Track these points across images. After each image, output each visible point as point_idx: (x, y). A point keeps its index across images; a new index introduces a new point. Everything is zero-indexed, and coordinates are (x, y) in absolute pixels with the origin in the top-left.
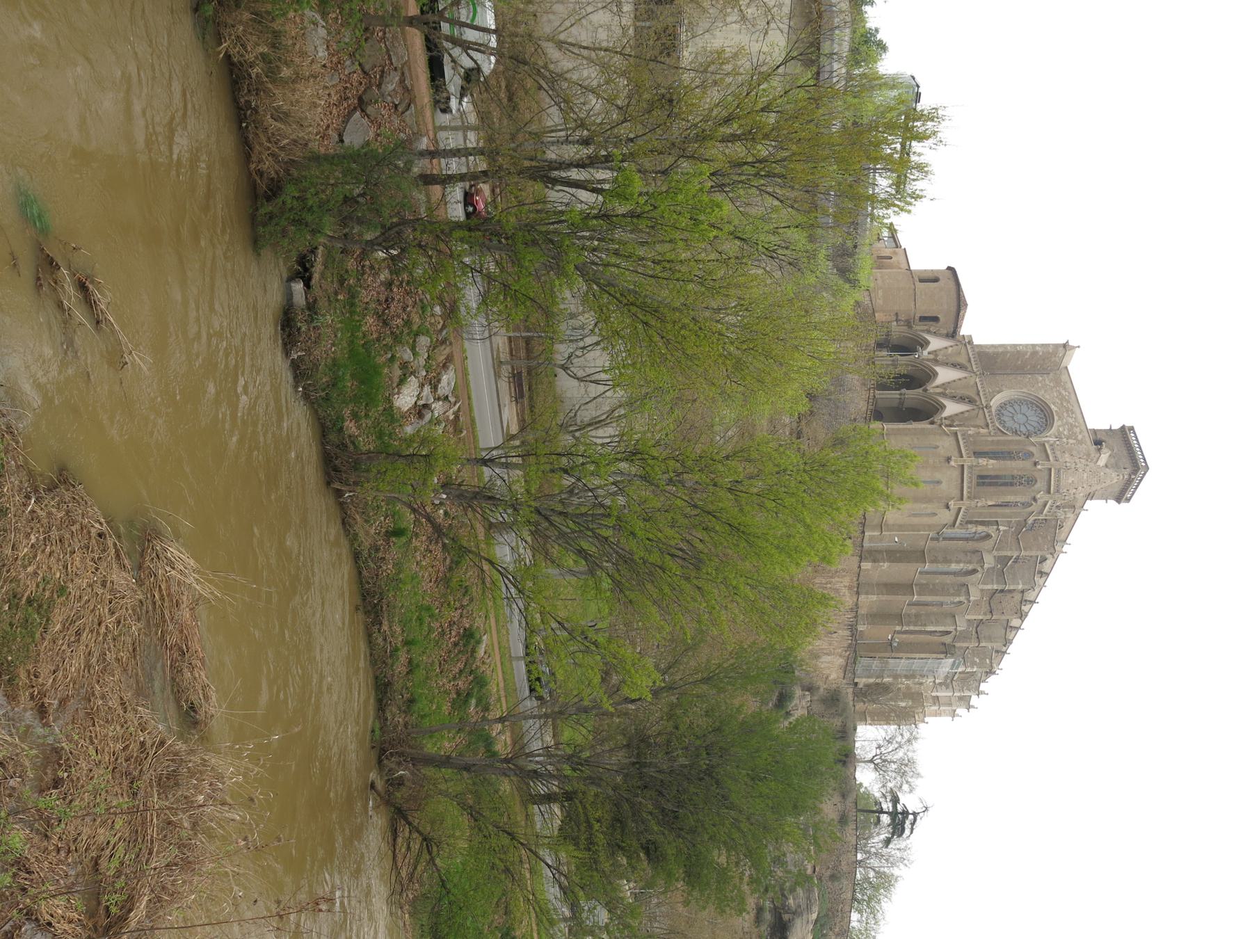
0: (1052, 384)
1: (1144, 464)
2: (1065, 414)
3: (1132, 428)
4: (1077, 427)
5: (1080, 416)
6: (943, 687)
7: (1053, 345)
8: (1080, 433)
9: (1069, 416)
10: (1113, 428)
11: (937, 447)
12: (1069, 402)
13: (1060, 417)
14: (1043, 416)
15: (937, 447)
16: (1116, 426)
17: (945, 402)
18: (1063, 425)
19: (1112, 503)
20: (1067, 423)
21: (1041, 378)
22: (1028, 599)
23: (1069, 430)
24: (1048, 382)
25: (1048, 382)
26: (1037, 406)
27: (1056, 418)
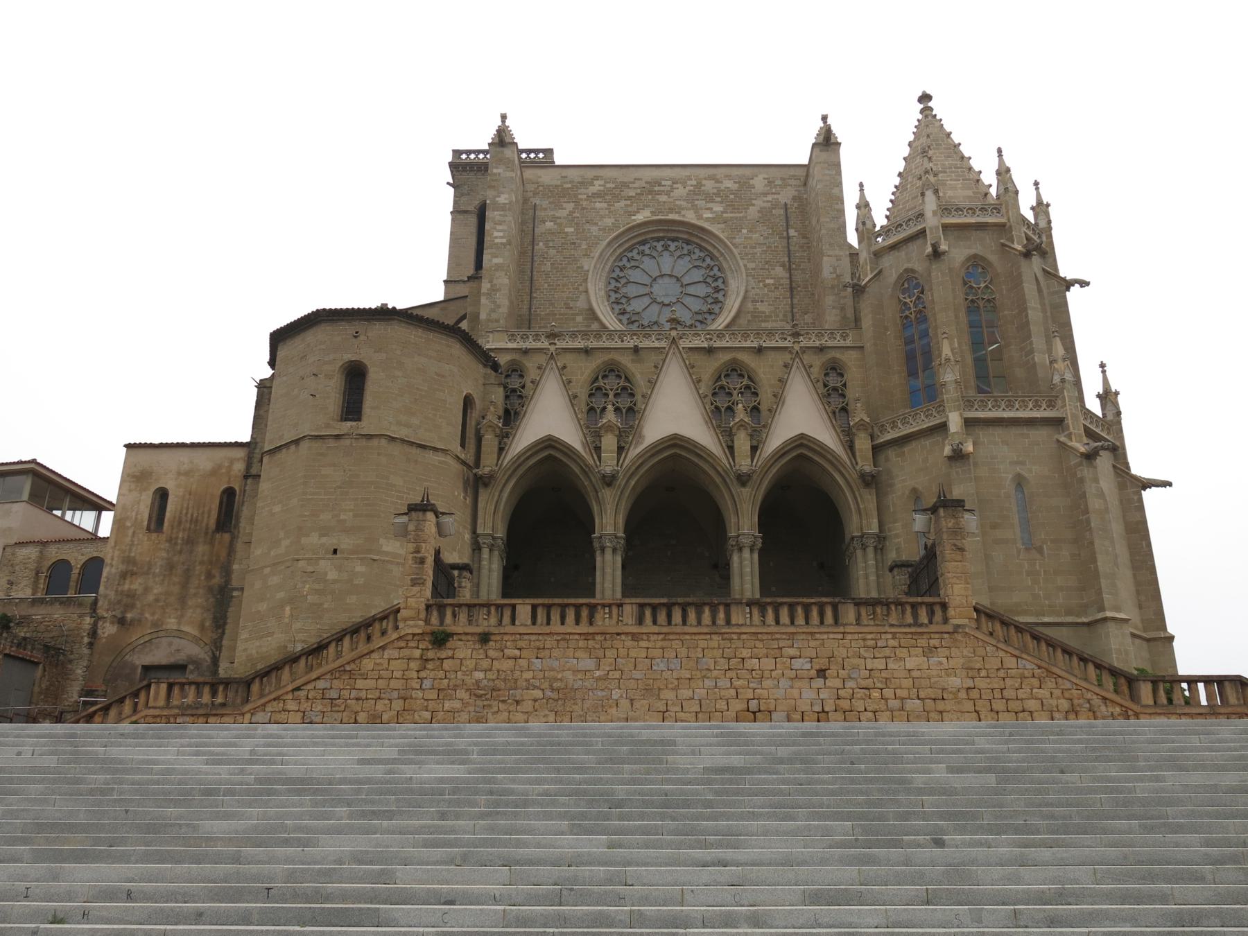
0: (570, 206)
1: (541, 155)
2: (663, 198)
3: (457, 153)
4: (699, 185)
5: (668, 172)
8: (717, 181)
9: (668, 193)
11: (1020, 482)
12: (625, 185)
13: (671, 211)
14: (659, 246)
15: (1020, 482)
18: (696, 209)
21: (549, 225)
23: (712, 201)
24: (562, 213)
25: (562, 213)
26: (630, 249)
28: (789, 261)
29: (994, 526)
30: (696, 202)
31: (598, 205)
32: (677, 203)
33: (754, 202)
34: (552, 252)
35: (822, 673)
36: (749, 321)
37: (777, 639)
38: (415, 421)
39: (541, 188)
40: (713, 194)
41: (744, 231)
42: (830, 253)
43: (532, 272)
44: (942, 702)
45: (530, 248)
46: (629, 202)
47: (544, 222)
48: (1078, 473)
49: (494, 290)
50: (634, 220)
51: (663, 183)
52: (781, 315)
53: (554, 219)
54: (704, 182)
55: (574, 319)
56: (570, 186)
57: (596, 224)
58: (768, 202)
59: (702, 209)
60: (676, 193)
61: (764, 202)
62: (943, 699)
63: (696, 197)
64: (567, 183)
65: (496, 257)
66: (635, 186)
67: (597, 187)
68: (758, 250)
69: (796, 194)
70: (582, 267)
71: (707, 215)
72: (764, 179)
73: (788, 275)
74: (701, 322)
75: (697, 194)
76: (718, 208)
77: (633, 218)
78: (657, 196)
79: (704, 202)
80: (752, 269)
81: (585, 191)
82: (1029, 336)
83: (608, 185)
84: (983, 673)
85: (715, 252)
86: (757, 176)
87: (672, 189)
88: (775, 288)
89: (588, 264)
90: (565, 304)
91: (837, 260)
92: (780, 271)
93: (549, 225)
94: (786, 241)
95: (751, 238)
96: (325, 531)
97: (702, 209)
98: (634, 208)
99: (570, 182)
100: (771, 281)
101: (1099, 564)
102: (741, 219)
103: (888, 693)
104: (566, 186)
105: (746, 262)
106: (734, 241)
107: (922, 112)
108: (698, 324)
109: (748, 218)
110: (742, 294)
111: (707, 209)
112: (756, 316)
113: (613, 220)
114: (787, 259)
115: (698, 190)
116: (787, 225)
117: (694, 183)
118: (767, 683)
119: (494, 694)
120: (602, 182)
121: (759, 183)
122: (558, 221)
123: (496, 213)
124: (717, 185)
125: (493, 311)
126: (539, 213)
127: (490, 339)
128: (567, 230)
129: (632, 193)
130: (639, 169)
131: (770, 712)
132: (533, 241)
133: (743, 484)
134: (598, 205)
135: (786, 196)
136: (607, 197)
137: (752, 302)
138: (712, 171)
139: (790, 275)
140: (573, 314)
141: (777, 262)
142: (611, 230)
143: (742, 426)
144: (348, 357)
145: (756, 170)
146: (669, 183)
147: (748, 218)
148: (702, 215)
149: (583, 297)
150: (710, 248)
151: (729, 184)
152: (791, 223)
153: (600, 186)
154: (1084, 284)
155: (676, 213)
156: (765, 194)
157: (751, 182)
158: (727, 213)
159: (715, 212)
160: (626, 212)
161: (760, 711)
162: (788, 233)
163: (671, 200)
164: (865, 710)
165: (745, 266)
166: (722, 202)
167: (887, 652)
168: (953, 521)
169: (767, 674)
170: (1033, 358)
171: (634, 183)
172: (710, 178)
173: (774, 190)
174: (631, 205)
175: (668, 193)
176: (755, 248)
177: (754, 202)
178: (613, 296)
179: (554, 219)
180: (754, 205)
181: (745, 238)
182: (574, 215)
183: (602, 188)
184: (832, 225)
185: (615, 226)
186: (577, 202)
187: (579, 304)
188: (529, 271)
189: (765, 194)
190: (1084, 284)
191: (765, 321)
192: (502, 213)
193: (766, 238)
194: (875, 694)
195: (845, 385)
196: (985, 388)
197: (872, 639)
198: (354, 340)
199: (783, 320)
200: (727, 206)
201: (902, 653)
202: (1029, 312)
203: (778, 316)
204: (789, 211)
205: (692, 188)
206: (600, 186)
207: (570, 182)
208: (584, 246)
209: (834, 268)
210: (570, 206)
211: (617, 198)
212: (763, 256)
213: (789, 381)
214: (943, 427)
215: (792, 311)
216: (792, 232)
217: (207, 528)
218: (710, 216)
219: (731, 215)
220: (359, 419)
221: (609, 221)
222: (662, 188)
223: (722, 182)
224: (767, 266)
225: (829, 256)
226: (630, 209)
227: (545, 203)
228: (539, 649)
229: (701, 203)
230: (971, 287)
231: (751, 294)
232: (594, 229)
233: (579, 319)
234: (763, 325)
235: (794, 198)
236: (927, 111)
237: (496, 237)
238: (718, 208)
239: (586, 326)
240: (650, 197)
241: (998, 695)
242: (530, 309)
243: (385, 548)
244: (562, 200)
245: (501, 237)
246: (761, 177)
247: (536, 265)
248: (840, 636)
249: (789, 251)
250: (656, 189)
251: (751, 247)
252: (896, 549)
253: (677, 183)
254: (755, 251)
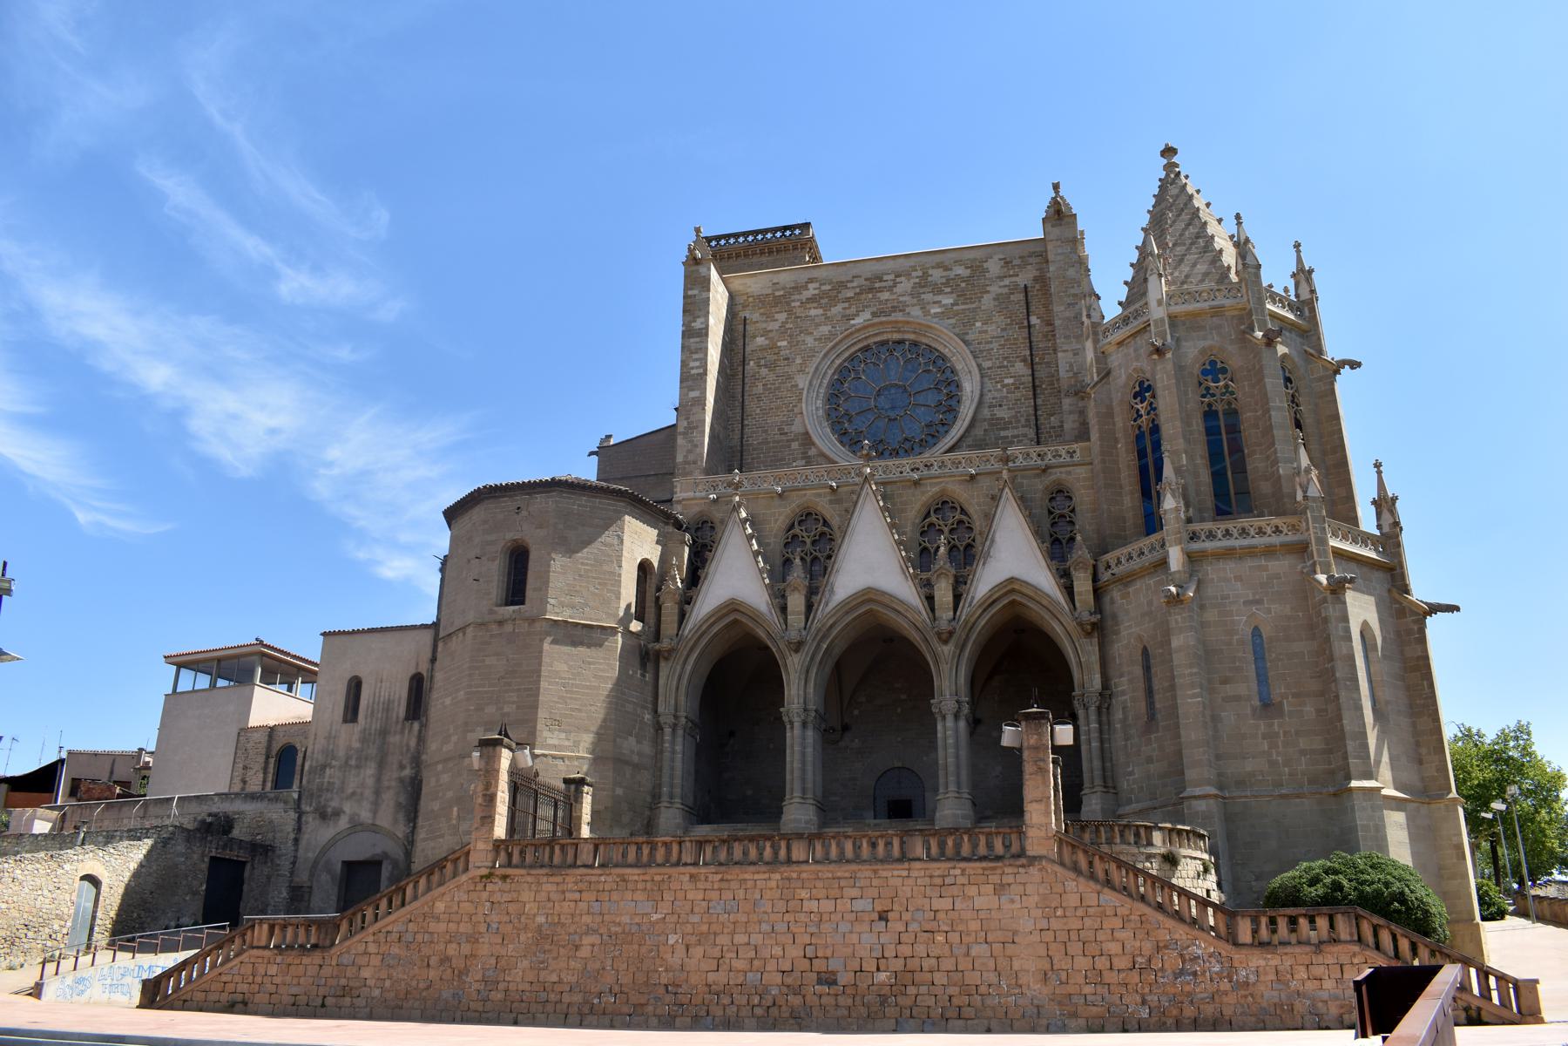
0: (782, 317)
2: (885, 296)
4: (925, 275)
5: (890, 265)
7: (685, 290)
8: (947, 269)
9: (890, 289)
13: (894, 309)
17: (986, 580)
18: (924, 307)
20: (915, 293)
23: (940, 292)
27: (898, 316)
28: (1031, 355)
29: (1225, 681)
30: (923, 296)
31: (813, 312)
32: (901, 299)
33: (988, 288)
34: (764, 371)
35: (883, 917)
36: (985, 430)
37: (839, 878)
39: (751, 299)
40: (942, 284)
41: (978, 324)
42: (1065, 347)
43: (743, 396)
44: (1012, 945)
45: (740, 368)
46: (846, 305)
47: (755, 337)
48: (1323, 610)
49: (690, 428)
50: (854, 325)
51: (885, 278)
52: (1023, 420)
53: (765, 333)
54: (930, 272)
55: (789, 446)
56: (782, 293)
57: (812, 333)
58: (1006, 286)
59: (928, 303)
60: (899, 289)
61: (1000, 287)
62: (1013, 942)
63: (922, 290)
64: (778, 290)
65: (693, 390)
66: (855, 284)
67: (812, 290)
68: (995, 345)
69: (1037, 273)
70: (797, 385)
71: (935, 310)
72: (1000, 259)
73: (1030, 372)
74: (933, 436)
75: (924, 287)
76: (947, 300)
77: (852, 322)
78: (879, 295)
79: (931, 295)
80: (989, 368)
81: (797, 297)
82: (1273, 444)
83: (824, 288)
84: (1059, 913)
85: (945, 351)
86: (991, 258)
87: (895, 285)
88: (1016, 388)
89: (802, 381)
90: (779, 430)
91: (1075, 355)
92: (1021, 368)
93: (760, 341)
94: (1027, 330)
95: (986, 332)
97: (928, 303)
98: (853, 310)
99: (783, 289)
100: (1010, 381)
101: (1344, 722)
102: (974, 310)
103: (954, 937)
104: (777, 294)
105: (980, 360)
106: (967, 338)
107: (1165, 168)
108: (929, 438)
109: (983, 307)
110: (976, 400)
111: (934, 303)
112: (996, 423)
113: (829, 328)
114: (1028, 353)
115: (924, 283)
116: (1028, 312)
117: (920, 273)
118: (826, 927)
119: (555, 938)
120: (816, 285)
121: (994, 267)
122: (771, 335)
123: (692, 340)
124: (945, 274)
125: (690, 451)
127: (678, 490)
128: (779, 344)
129: (850, 294)
130: (858, 265)
131: (827, 958)
132: (744, 361)
133: (946, 642)
134: (813, 312)
135: (1025, 277)
136: (823, 301)
137: (989, 407)
138: (938, 258)
139: (1033, 371)
140: (788, 441)
141: (1017, 357)
142: (828, 339)
143: (942, 573)
144: (510, 536)
145: (989, 250)
146: (892, 277)
147: (983, 307)
148: (929, 311)
149: (798, 421)
150: (940, 348)
151: (960, 271)
152: (1032, 308)
153: (815, 289)
154: (1354, 365)
155: (900, 311)
156: (1001, 278)
157: (985, 265)
158: (957, 304)
159: (947, 305)
160: (843, 316)
161: (817, 957)
162: (1029, 322)
163: (895, 297)
164: (928, 956)
165: (979, 366)
166: (952, 293)
167: (955, 890)
168: (1035, 737)
169: (825, 917)
170: (1278, 471)
171: (852, 281)
172: (938, 266)
173: (1011, 273)
174: (850, 308)
175: (890, 289)
176: (991, 342)
177: (988, 288)
178: (834, 415)
179: (765, 333)
180: (988, 292)
181: (980, 332)
182: (787, 326)
183: (817, 292)
184: (1067, 314)
185: (832, 335)
186: (790, 312)
187: (793, 428)
188: (740, 396)
189: (1001, 278)
190: (1354, 365)
191: (1004, 429)
192: (698, 339)
193: (1003, 330)
194: (939, 938)
195: (1073, 511)
196: (1223, 507)
197: (939, 876)
198: (516, 516)
199: (1026, 426)
200: (958, 296)
201: (972, 891)
202: (1273, 413)
203: (1019, 421)
204: (1030, 294)
205: (917, 280)
206: (815, 289)
207: (783, 289)
208: (798, 361)
209: (1071, 365)
210: (782, 317)
211: (834, 301)
212: (1001, 352)
213: (997, 516)
214: (1163, 563)
215: (1036, 415)
216: (1034, 320)
217: (398, 717)
218: (939, 310)
219: (963, 307)
220: (523, 603)
221: (825, 329)
222: (883, 284)
223: (951, 269)
224: (1005, 363)
225: (1064, 351)
226: (848, 312)
227: (756, 316)
228: (598, 891)
229: (928, 297)
230: (1208, 389)
231: (988, 398)
232: (810, 340)
233: (795, 445)
234: (1003, 433)
235: (1036, 279)
236: (1170, 167)
237: (692, 368)
238: (947, 300)
239: (802, 453)
240: (870, 296)
241: (1074, 936)
242: (742, 438)
243: (550, 741)
244: (773, 310)
245: (697, 367)
246: (996, 258)
247: (747, 388)
248: (905, 873)
249: (1030, 342)
250: (877, 285)
251: (987, 343)
252: (1123, 708)
253: (898, 276)
254: (991, 346)
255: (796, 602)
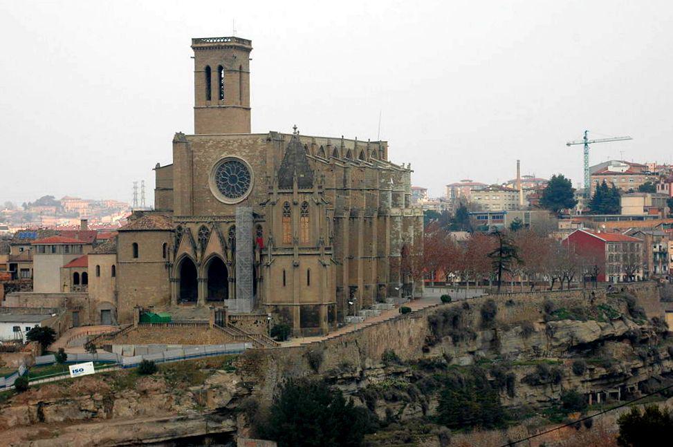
6: (398, 198)
10: (194, 56)
12: (219, 142)
16: (192, 53)
19: (251, 55)
21: (197, 158)
22: (340, 145)
38: (150, 256)
53: (198, 156)
67: (211, 143)
71: (244, 154)
89: (209, 173)
93: (197, 158)
96: (133, 285)
126: (194, 154)
145: (258, 136)
179: (198, 156)
229: (242, 150)
255: (199, 254)
